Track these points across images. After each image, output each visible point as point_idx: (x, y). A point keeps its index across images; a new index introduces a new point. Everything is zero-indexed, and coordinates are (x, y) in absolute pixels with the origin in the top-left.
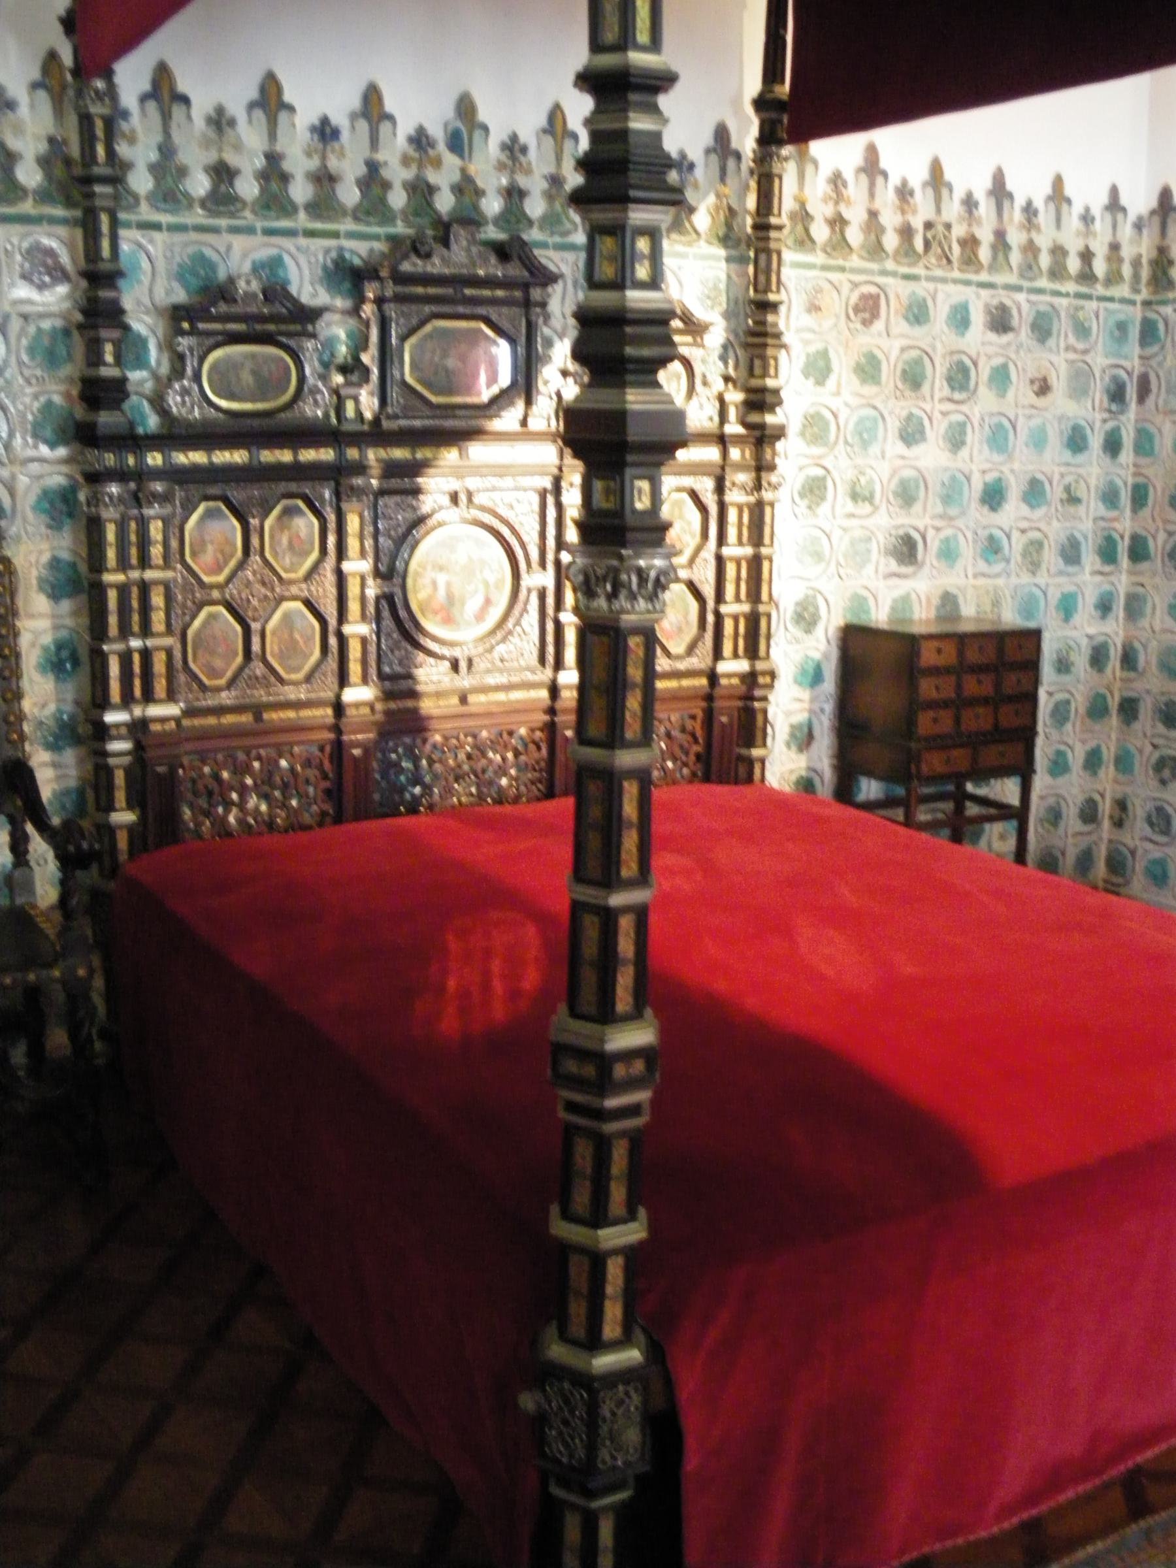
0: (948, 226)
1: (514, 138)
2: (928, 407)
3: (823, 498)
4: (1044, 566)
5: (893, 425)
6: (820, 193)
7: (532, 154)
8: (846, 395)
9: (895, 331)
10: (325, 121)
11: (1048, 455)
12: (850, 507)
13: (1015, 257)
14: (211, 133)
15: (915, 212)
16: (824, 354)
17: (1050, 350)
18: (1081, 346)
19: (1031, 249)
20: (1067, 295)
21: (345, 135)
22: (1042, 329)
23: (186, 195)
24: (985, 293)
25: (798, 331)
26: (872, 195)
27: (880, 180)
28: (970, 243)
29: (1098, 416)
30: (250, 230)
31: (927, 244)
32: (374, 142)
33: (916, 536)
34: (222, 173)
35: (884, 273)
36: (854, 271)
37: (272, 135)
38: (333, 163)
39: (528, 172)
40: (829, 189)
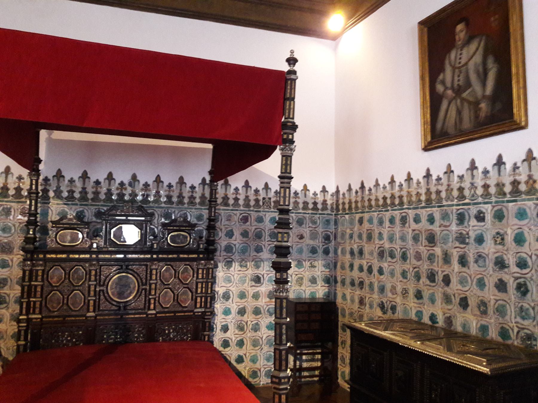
0: (270, 199)
1: (146, 183)
2: (263, 243)
3: (231, 266)
4: (304, 284)
5: (253, 248)
6: (231, 192)
7: (151, 187)
8: (238, 241)
9: (253, 225)
10: (97, 180)
11: (304, 255)
12: (240, 268)
14: (69, 183)
15: (260, 196)
16: (232, 231)
20: (308, 214)
21: (102, 184)
23: (62, 197)
25: (224, 225)
26: (247, 192)
27: (249, 189)
29: (321, 244)
30: (77, 204)
31: (263, 203)
32: (110, 184)
33: (261, 276)
34: (71, 192)
36: (241, 210)
37: (84, 183)
38: (99, 189)
39: (150, 190)
40: (234, 191)
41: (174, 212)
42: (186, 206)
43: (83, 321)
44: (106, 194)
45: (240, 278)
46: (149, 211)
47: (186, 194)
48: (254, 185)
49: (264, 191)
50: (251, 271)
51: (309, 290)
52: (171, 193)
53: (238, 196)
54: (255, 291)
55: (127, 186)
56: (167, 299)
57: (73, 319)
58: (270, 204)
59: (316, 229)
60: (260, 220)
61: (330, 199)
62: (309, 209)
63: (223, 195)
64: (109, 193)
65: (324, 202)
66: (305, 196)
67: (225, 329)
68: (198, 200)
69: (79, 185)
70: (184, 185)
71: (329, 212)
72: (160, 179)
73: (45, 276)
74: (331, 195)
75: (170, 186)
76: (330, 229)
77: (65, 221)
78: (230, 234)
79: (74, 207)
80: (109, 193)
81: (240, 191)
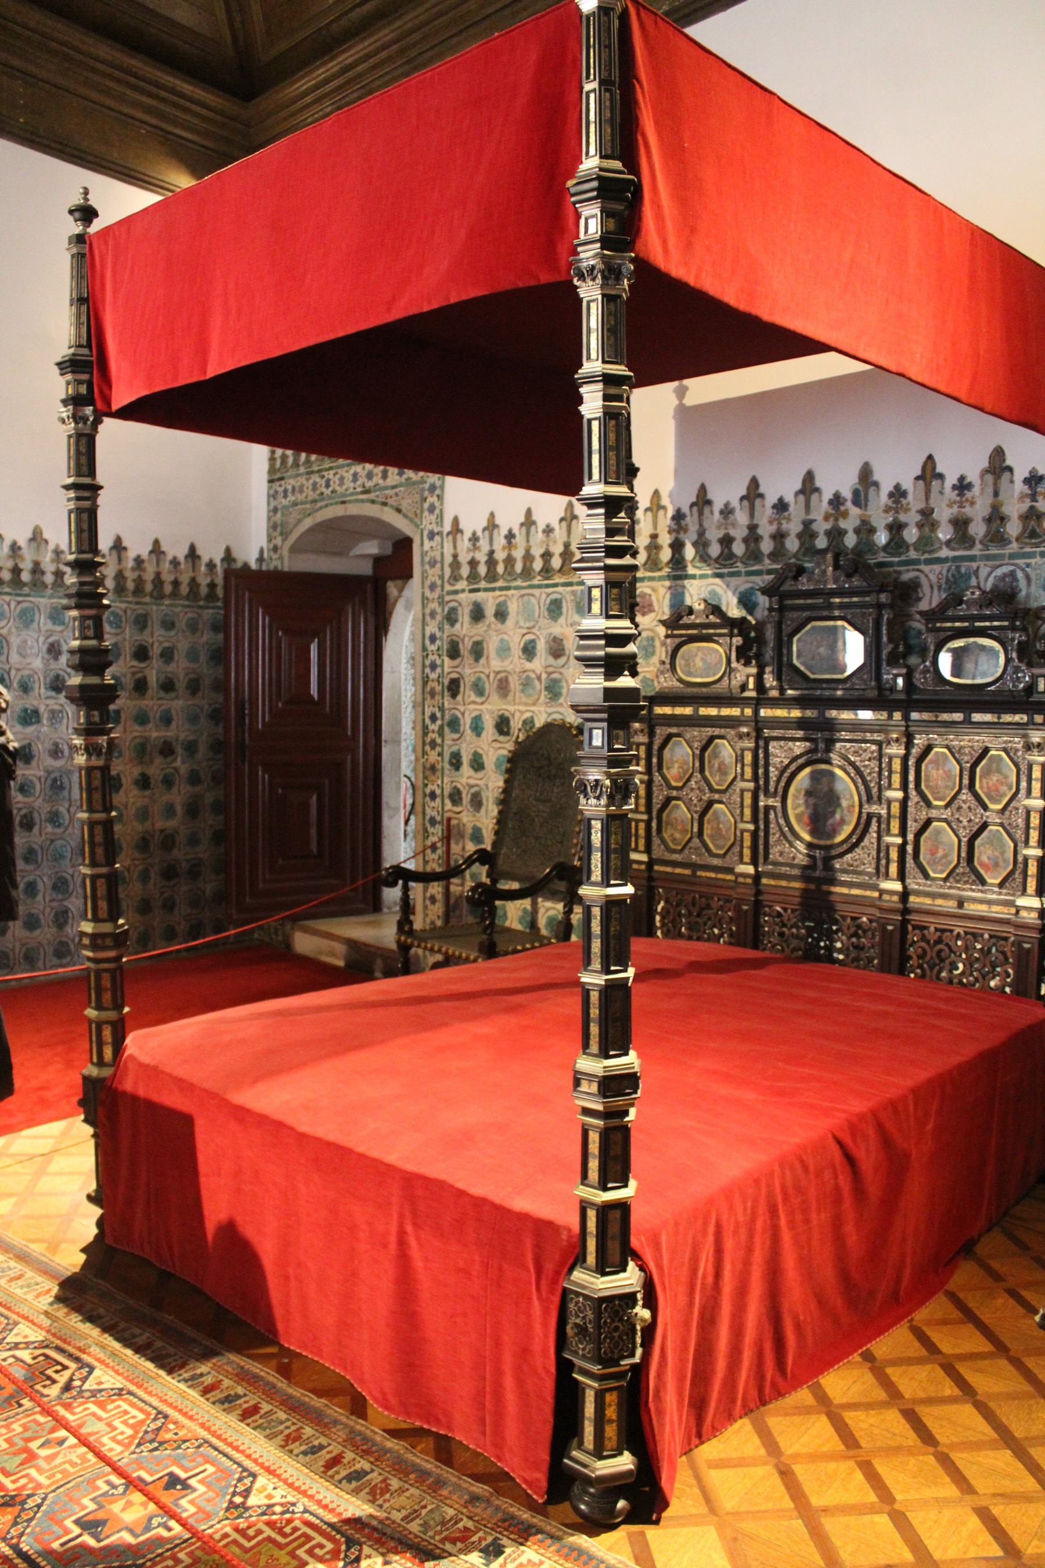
7: (910, 497)
21: (791, 508)
23: (709, 556)
34: (726, 541)
37: (752, 515)
38: (785, 526)
39: (907, 510)
41: (976, 572)
42: (1014, 546)
43: (869, 903)
44: (799, 536)
46: (906, 577)
52: (968, 510)
55: (849, 504)
56: (940, 853)
57: (713, 875)
64: (807, 533)
69: (741, 518)
70: (1006, 475)
72: (934, 468)
73: (655, 760)
75: (962, 486)
79: (733, 580)
80: (807, 533)
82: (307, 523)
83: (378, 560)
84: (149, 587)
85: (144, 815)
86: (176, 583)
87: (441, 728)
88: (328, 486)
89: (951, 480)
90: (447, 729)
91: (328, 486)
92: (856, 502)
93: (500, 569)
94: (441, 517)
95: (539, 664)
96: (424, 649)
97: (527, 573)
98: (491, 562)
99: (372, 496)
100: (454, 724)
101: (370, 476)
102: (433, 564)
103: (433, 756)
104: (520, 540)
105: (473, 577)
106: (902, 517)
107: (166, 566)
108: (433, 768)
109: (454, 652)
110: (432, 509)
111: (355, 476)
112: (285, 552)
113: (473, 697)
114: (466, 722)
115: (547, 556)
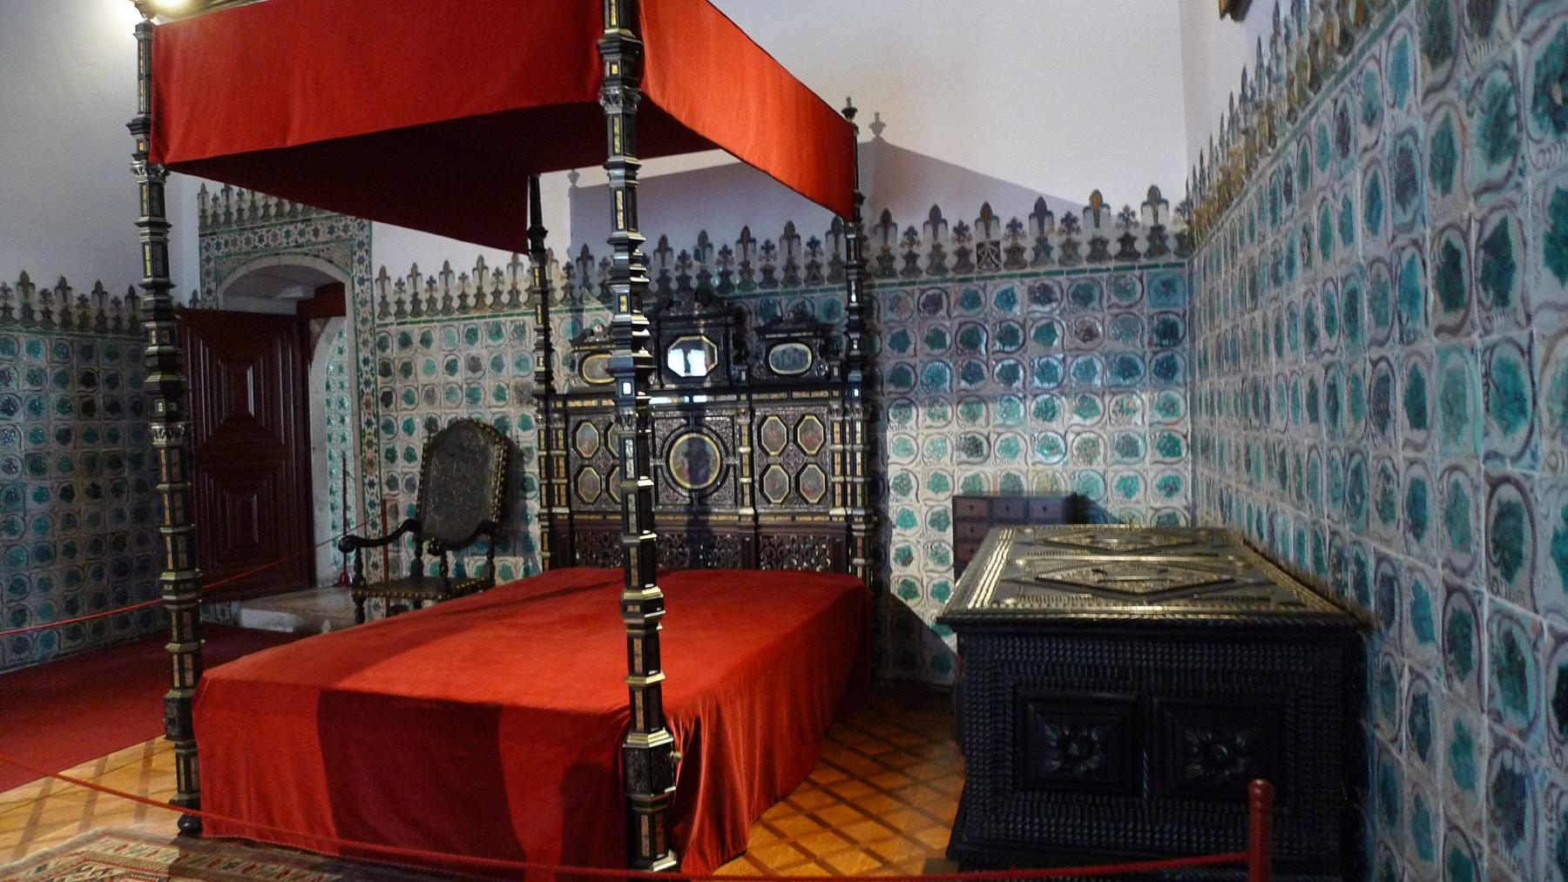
0: (997, 244)
1: (725, 247)
3: (909, 418)
4: (1100, 458)
12: (929, 422)
13: (1056, 254)
15: (970, 239)
16: (904, 333)
17: (1093, 309)
18: (1125, 303)
19: (1070, 247)
20: (1108, 270)
22: (1083, 296)
24: (1027, 281)
26: (935, 236)
27: (941, 227)
28: (1015, 252)
35: (946, 281)
42: (803, 286)
45: (932, 443)
47: (802, 261)
48: (951, 217)
49: (981, 225)
50: (955, 426)
51: (1117, 472)
52: (772, 263)
53: (915, 250)
54: (968, 474)
58: (998, 256)
59: (1134, 310)
60: (972, 300)
61: (1175, 222)
62: (1111, 258)
63: (879, 253)
65: (1157, 231)
66: (1097, 225)
67: (906, 558)
68: (826, 271)
71: (1173, 258)
74: (1178, 210)
75: (768, 247)
76: (1175, 305)
77: (591, 339)
78: (901, 342)
81: (920, 236)
82: (242, 271)
83: (301, 303)
84: (93, 322)
85: (94, 520)
86: (118, 319)
87: (377, 431)
88: (261, 240)
89: (760, 243)
90: (382, 432)
91: (261, 240)
92: (697, 257)
93: (424, 307)
94: (369, 268)
95: (458, 378)
96: (358, 369)
97: (447, 309)
98: (416, 301)
99: (305, 250)
100: (388, 427)
101: (302, 233)
102: (363, 303)
103: (370, 453)
104: (439, 284)
105: (400, 313)
106: (729, 268)
107: (108, 305)
108: (371, 463)
109: (386, 370)
110: (361, 261)
111: (288, 234)
112: (220, 295)
113: (404, 405)
114: (399, 425)
115: (463, 297)
